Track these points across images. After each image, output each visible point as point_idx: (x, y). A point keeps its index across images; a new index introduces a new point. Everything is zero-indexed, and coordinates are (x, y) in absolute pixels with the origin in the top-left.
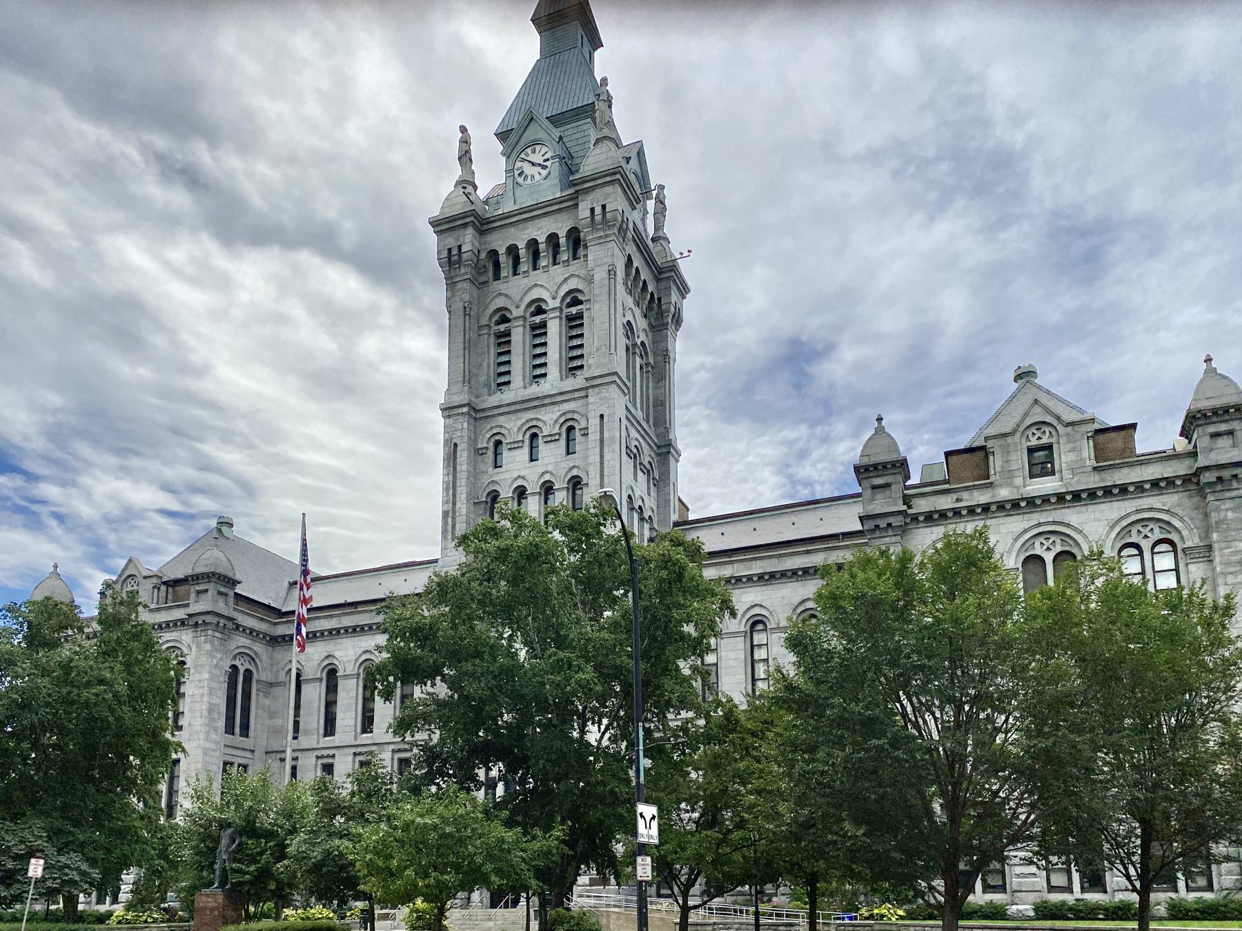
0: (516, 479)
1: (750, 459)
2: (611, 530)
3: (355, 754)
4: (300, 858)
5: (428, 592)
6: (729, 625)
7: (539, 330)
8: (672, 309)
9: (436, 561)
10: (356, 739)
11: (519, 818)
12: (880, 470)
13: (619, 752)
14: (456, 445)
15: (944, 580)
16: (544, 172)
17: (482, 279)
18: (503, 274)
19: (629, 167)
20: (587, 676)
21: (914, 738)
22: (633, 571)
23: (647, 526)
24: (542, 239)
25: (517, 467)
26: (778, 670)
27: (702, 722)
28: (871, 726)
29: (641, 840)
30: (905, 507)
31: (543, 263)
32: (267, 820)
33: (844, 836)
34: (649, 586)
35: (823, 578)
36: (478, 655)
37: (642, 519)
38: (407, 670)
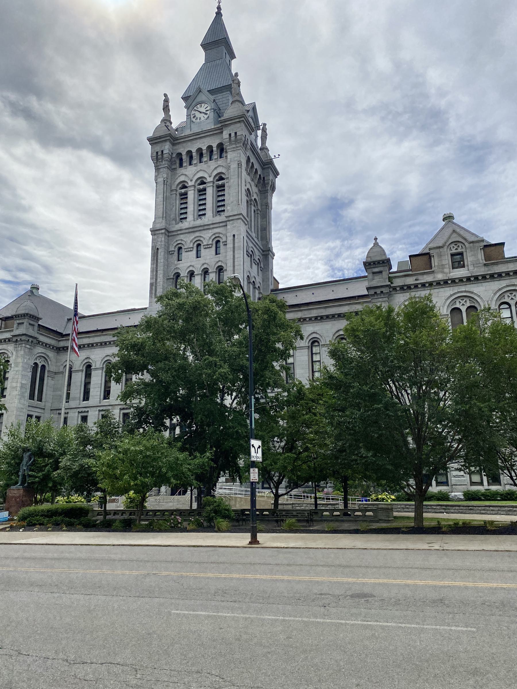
0: (189, 267)
1: (311, 257)
2: (238, 294)
3: (99, 411)
4: (67, 469)
5: (141, 325)
6: (299, 343)
7: (202, 192)
8: (270, 183)
9: (146, 309)
10: (100, 403)
11: (187, 446)
12: (376, 264)
13: (242, 410)
14: (158, 249)
15: (410, 321)
16: (206, 116)
17: (173, 167)
18: (184, 164)
19: (248, 114)
20: (225, 371)
21: (397, 404)
22: (249, 316)
23: (257, 292)
24: (204, 148)
25: (189, 261)
26: (325, 368)
27: (286, 394)
28: (373, 398)
29: (253, 459)
30: (389, 283)
31: (205, 159)
32: (50, 447)
33: (361, 456)
34: (258, 323)
35: (347, 320)
36: (166, 358)
37: (254, 288)
38: (130, 367)
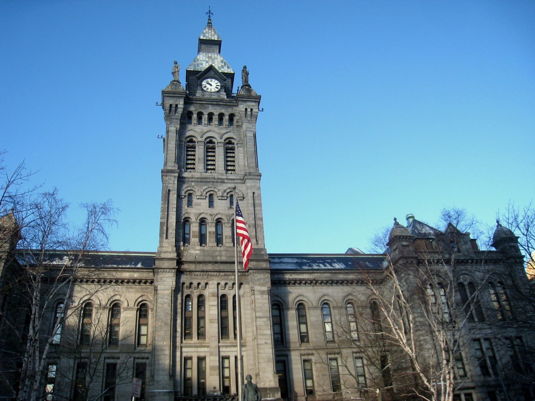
14: (169, 190)
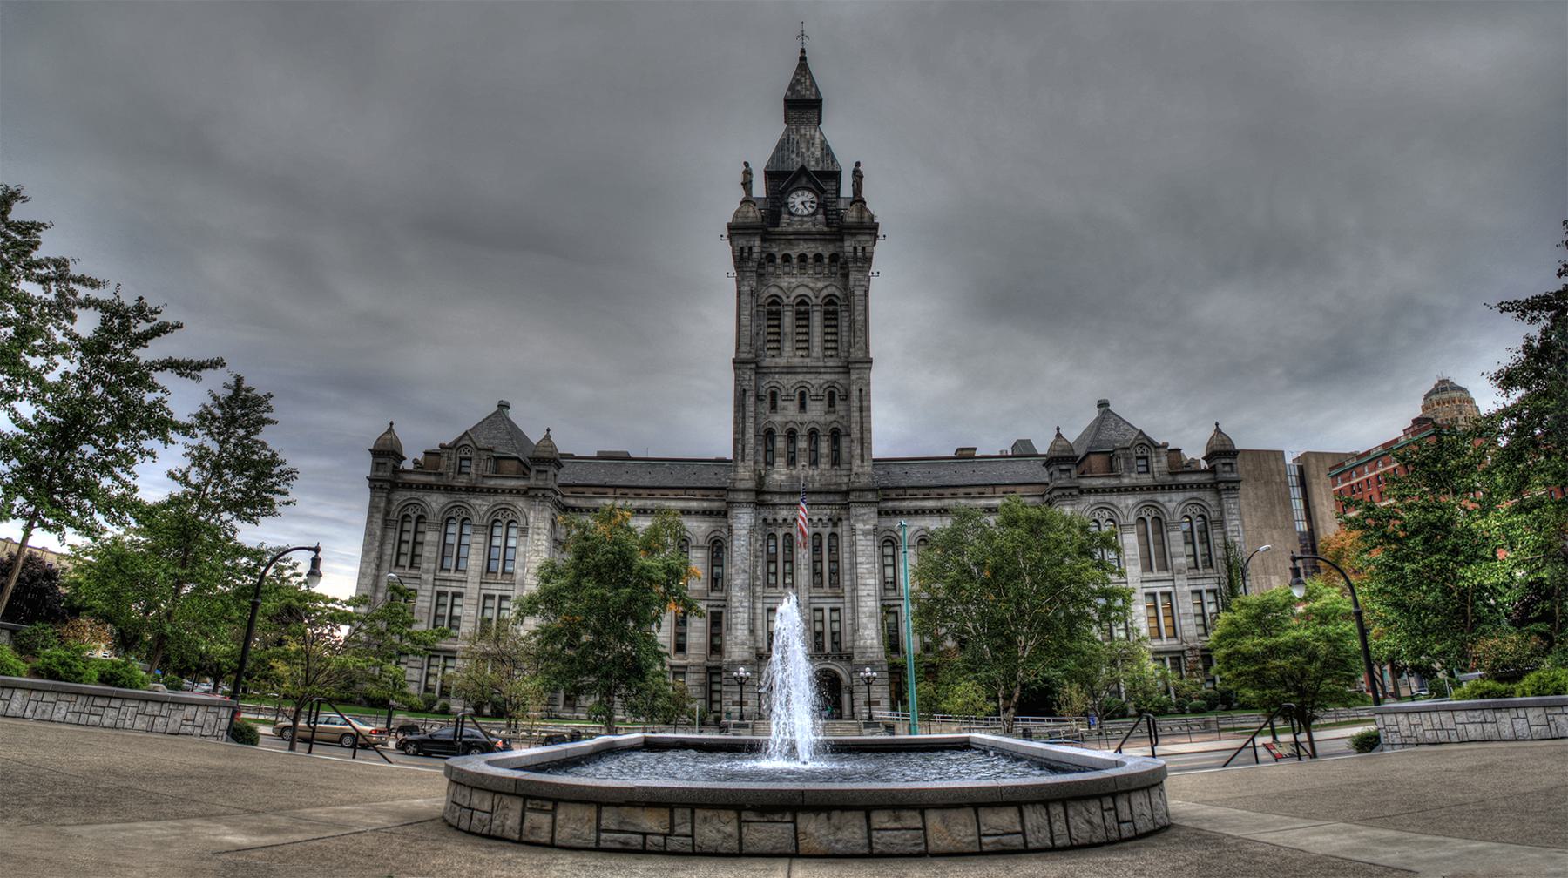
7: (803, 316)
